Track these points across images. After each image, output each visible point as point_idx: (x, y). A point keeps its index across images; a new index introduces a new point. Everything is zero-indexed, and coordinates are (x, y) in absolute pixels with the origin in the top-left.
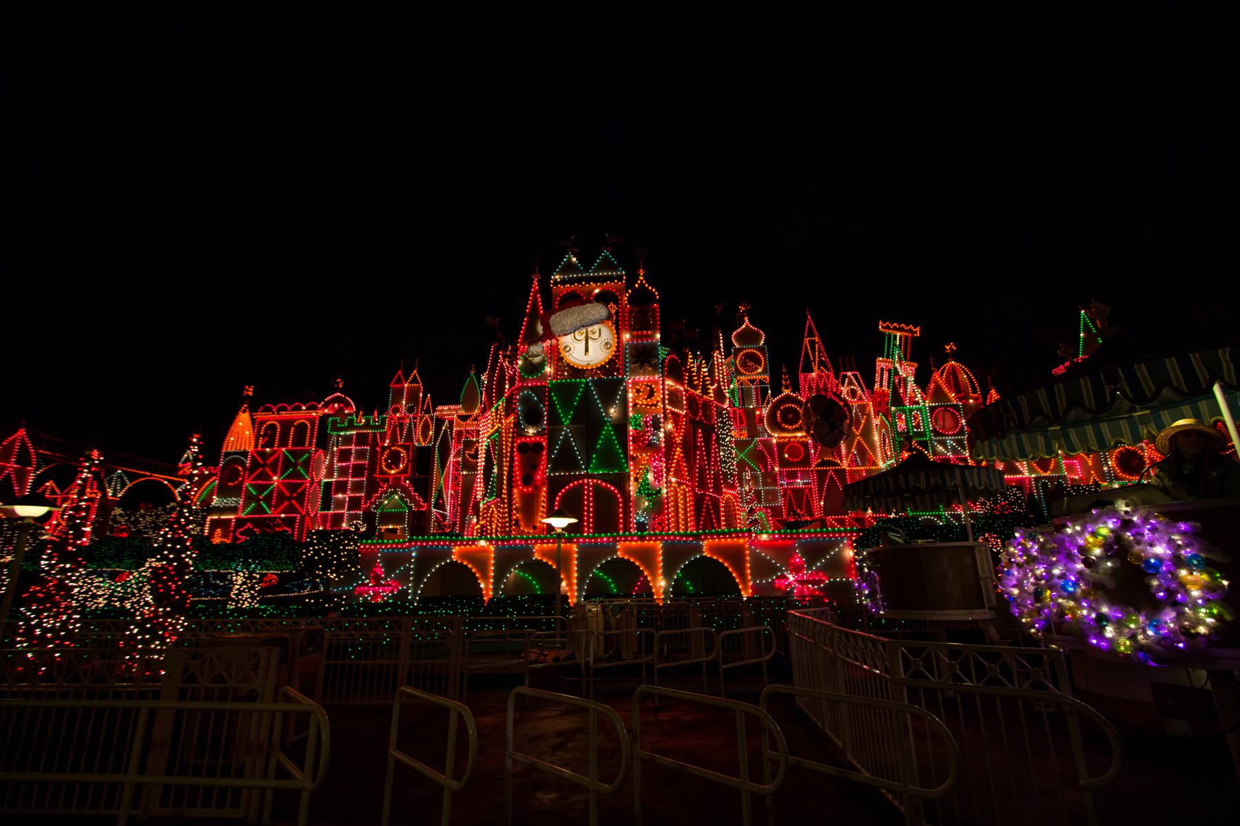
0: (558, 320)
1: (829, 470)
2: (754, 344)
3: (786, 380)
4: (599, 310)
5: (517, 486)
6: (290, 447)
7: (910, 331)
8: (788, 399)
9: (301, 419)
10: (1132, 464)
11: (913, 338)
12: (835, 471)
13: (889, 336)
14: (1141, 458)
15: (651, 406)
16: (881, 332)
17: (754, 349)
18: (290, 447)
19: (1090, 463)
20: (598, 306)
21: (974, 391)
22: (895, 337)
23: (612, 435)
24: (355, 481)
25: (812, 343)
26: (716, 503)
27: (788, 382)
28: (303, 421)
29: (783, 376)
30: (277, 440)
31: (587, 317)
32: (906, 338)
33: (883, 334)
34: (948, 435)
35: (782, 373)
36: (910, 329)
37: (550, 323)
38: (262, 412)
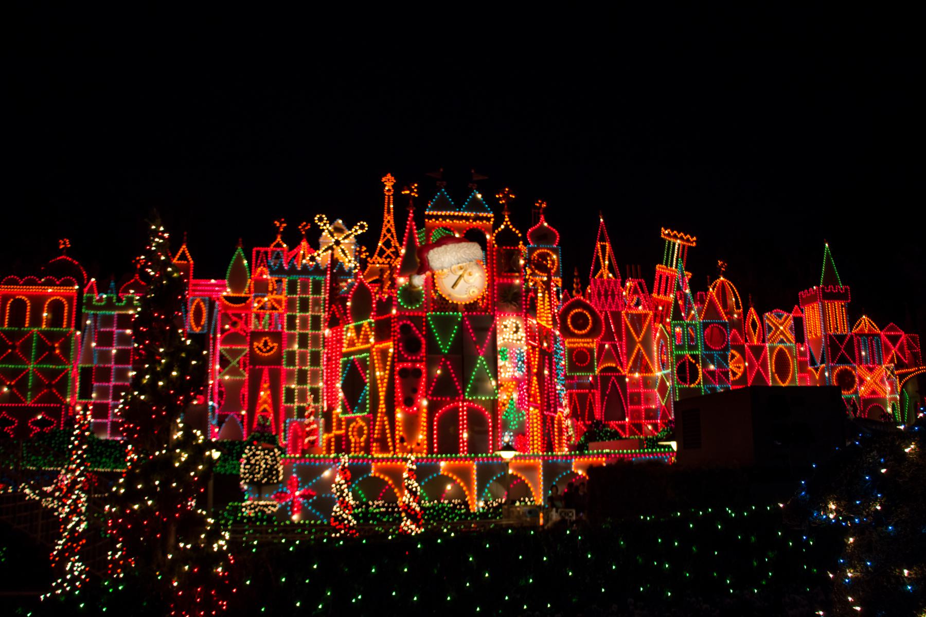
0: (437, 256)
1: (610, 377)
2: (547, 244)
3: (577, 284)
4: (473, 250)
5: (399, 405)
6: (44, 326)
7: (688, 240)
8: (579, 304)
9: (57, 296)
10: (847, 381)
11: (690, 247)
12: (617, 377)
13: (669, 242)
14: (853, 377)
15: (517, 340)
16: (663, 238)
17: (548, 249)
18: (44, 326)
19: (817, 377)
20: (474, 246)
21: (738, 308)
22: (674, 244)
23: (484, 365)
24: (119, 368)
25: (603, 248)
26: (553, 419)
27: (579, 286)
28: (58, 298)
29: (575, 280)
30: (8, 311)
31: (464, 256)
32: (684, 246)
33: (664, 241)
34: (716, 350)
35: (574, 276)
36: (688, 239)
37: (429, 258)
38: (5, 285)
